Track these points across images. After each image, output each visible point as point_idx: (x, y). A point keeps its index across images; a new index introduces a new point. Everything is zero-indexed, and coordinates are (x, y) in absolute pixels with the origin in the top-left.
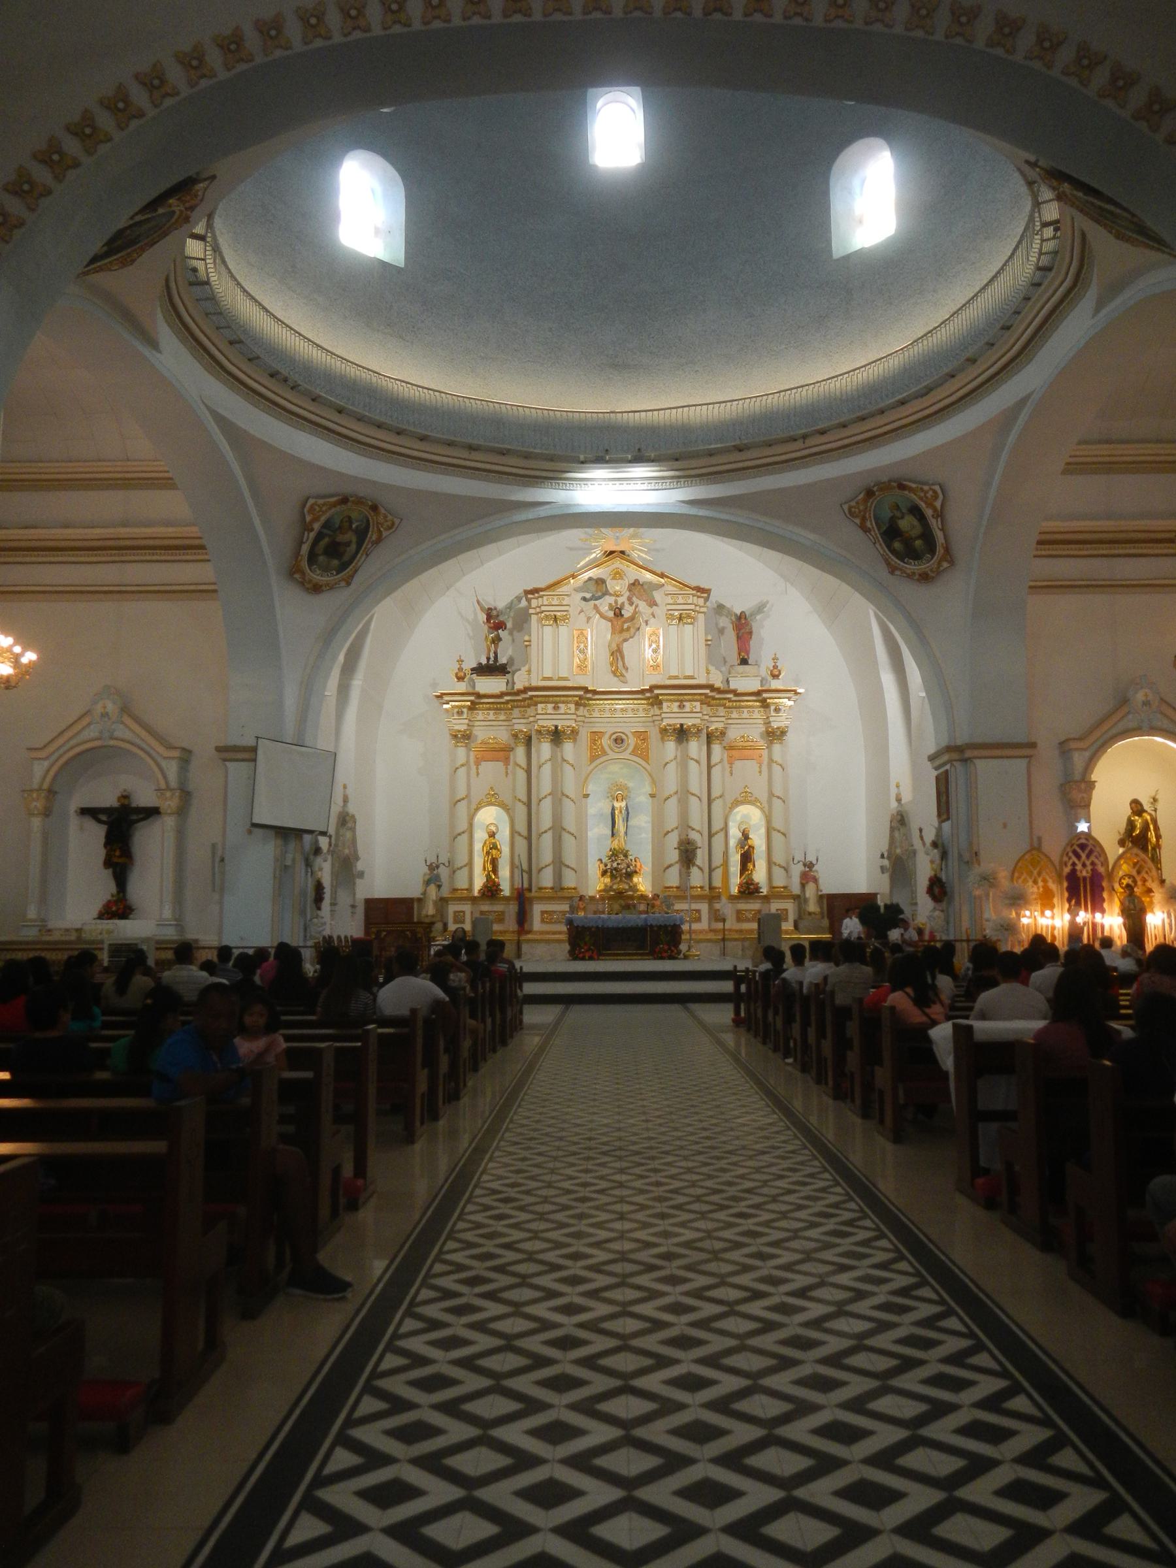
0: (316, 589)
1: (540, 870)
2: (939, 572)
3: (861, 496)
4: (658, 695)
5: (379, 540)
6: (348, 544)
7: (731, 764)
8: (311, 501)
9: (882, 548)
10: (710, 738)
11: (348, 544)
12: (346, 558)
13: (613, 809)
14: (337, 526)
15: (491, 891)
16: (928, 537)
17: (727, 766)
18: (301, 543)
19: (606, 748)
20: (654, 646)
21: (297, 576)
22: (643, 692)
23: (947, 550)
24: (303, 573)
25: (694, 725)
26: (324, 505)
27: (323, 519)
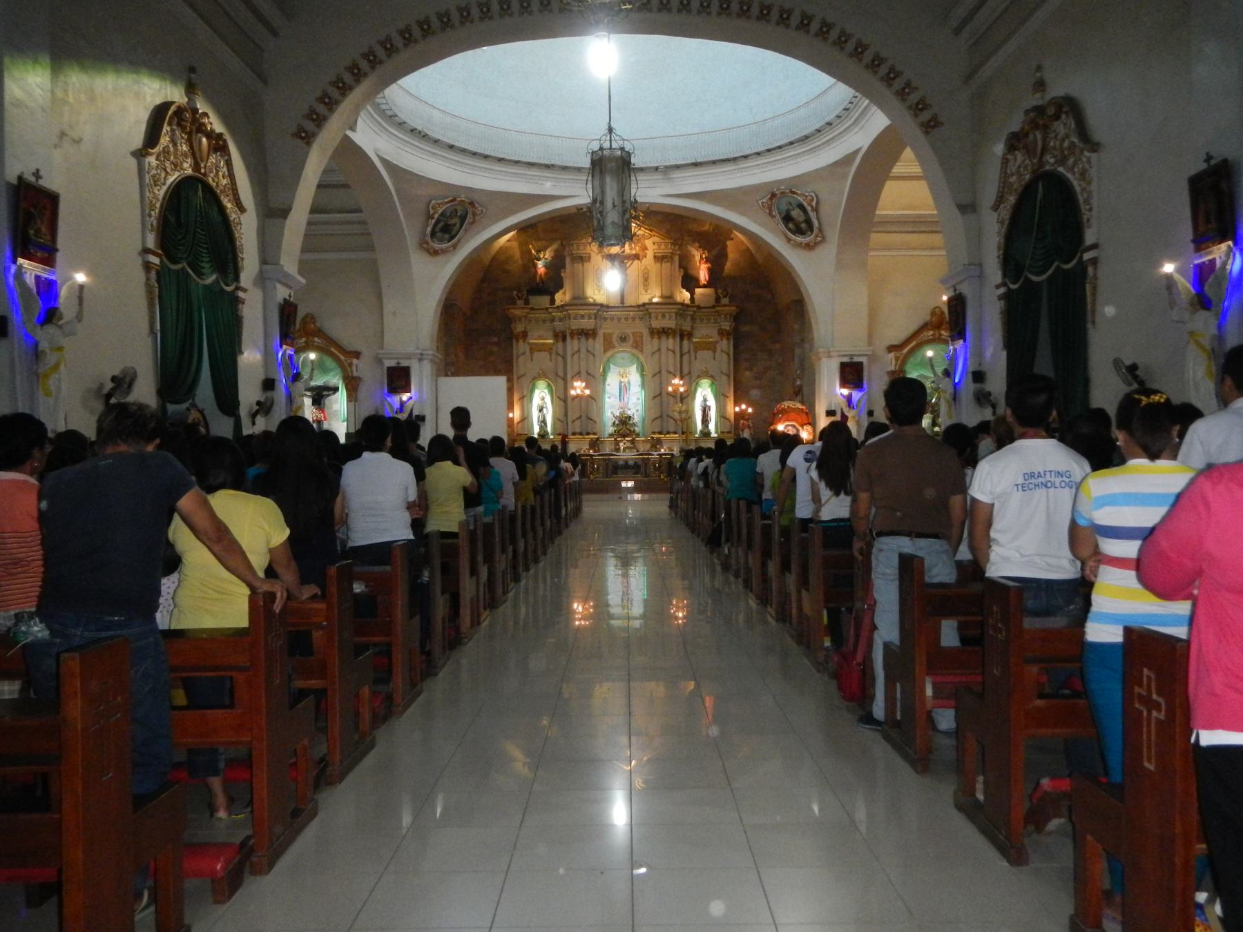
0: (435, 253)
1: (573, 421)
2: (816, 244)
3: (769, 196)
4: (648, 309)
5: (473, 223)
6: (455, 224)
7: (696, 352)
8: (434, 202)
9: (782, 226)
10: (682, 337)
11: (455, 224)
12: (453, 233)
13: (621, 382)
14: (448, 214)
15: (543, 435)
16: (808, 222)
17: (693, 354)
18: (428, 226)
19: (616, 344)
20: (646, 276)
21: (425, 246)
22: (639, 306)
23: (820, 230)
24: (427, 243)
25: (671, 329)
26: (442, 203)
27: (440, 212)
